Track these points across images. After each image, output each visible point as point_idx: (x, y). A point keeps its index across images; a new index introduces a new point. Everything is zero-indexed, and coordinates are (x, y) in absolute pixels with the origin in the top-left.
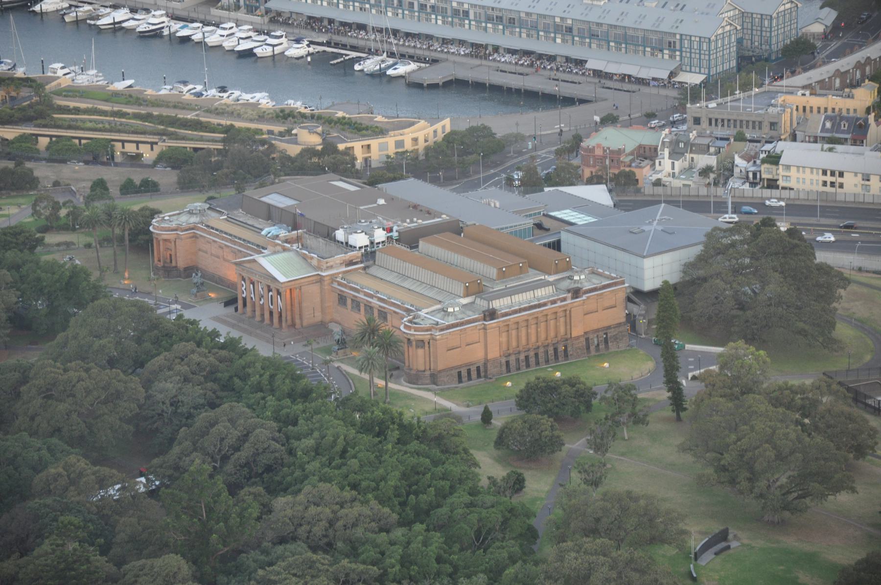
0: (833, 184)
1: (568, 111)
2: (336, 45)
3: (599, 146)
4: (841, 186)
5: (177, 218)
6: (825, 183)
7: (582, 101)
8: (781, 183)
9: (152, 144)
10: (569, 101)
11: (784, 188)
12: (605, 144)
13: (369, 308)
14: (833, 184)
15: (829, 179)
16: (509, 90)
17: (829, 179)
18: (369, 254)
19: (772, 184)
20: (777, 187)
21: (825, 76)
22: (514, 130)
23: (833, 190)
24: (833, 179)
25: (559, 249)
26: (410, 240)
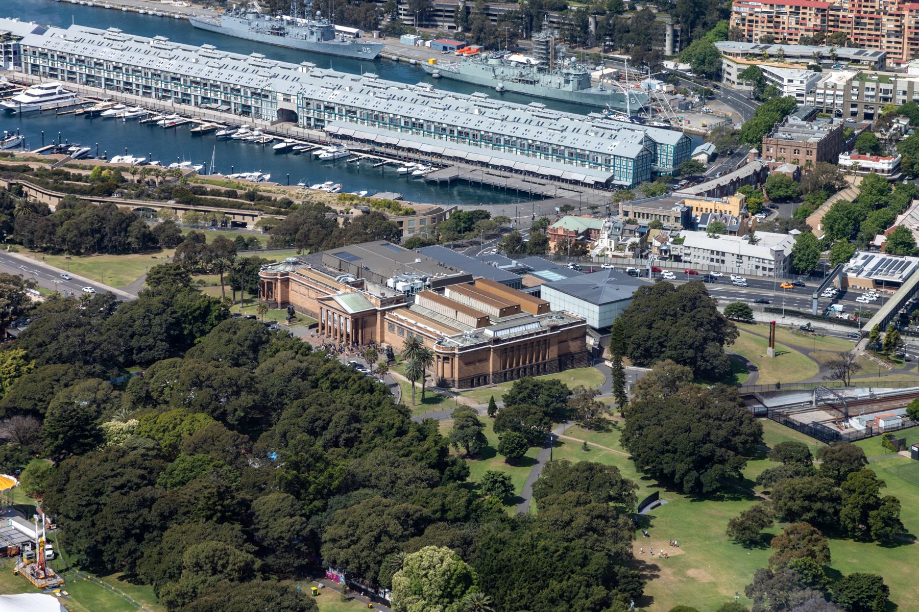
0: (717, 261)
1: (538, 204)
2: (377, 153)
3: (561, 228)
4: (723, 261)
5: (280, 263)
6: (712, 260)
7: (547, 197)
8: (684, 258)
9: (254, 216)
10: (538, 197)
11: (685, 262)
12: (565, 227)
13: (410, 331)
14: (717, 261)
15: (715, 257)
16: (496, 187)
17: (715, 257)
18: (409, 295)
19: (678, 259)
20: (681, 261)
21: (711, 188)
22: (501, 214)
23: (717, 264)
24: (718, 257)
25: (539, 297)
26: (439, 286)
